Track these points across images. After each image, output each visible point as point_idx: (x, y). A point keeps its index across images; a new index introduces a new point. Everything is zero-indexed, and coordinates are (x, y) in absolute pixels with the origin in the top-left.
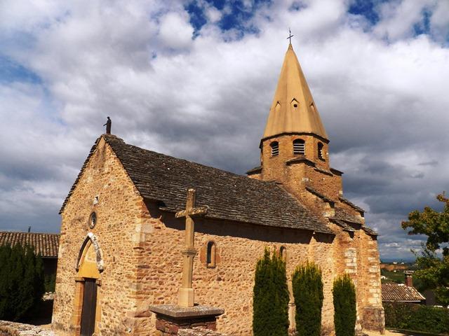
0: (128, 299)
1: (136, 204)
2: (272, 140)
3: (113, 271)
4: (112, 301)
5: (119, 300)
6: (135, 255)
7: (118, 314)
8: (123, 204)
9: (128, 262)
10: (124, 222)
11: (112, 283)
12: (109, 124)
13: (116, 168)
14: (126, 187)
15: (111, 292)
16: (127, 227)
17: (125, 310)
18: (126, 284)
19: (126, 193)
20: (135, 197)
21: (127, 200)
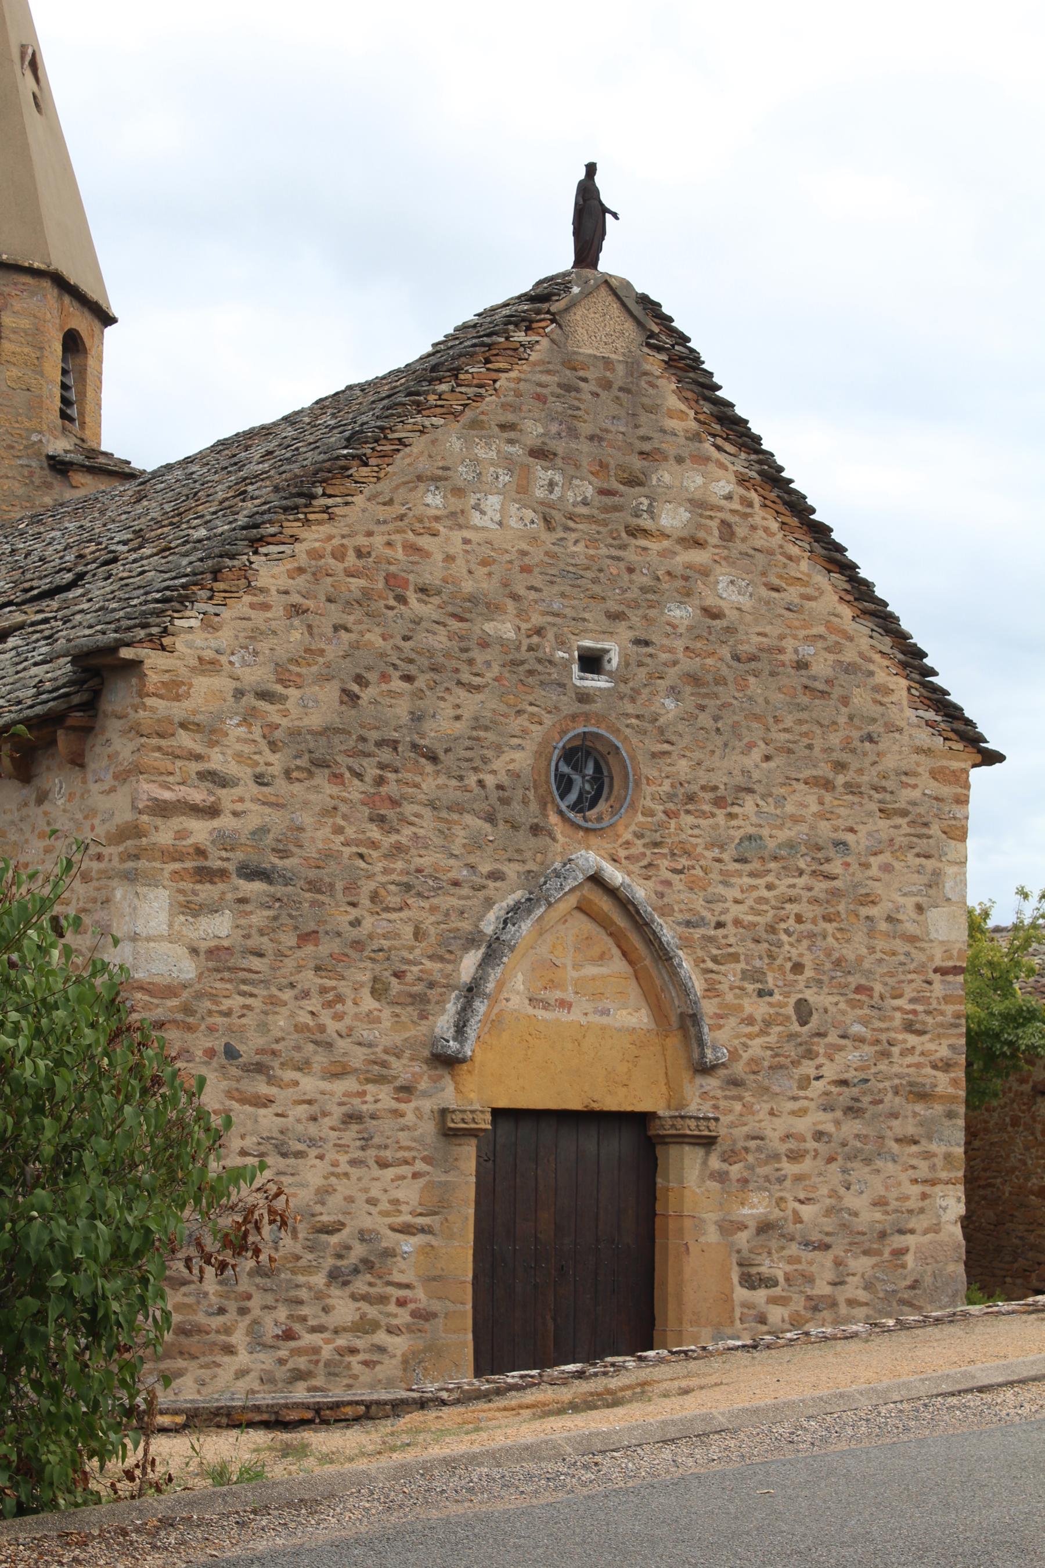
0: (916, 1190)
1: (934, 774)
3: (808, 1068)
4: (807, 1211)
5: (851, 1201)
6: (947, 999)
7: (861, 1264)
8: (848, 747)
9: (909, 1027)
11: (803, 1125)
13: (760, 540)
14: (850, 669)
15: (789, 1168)
16: (887, 868)
18: (910, 1129)
19: (861, 699)
20: (924, 737)
21: (870, 738)
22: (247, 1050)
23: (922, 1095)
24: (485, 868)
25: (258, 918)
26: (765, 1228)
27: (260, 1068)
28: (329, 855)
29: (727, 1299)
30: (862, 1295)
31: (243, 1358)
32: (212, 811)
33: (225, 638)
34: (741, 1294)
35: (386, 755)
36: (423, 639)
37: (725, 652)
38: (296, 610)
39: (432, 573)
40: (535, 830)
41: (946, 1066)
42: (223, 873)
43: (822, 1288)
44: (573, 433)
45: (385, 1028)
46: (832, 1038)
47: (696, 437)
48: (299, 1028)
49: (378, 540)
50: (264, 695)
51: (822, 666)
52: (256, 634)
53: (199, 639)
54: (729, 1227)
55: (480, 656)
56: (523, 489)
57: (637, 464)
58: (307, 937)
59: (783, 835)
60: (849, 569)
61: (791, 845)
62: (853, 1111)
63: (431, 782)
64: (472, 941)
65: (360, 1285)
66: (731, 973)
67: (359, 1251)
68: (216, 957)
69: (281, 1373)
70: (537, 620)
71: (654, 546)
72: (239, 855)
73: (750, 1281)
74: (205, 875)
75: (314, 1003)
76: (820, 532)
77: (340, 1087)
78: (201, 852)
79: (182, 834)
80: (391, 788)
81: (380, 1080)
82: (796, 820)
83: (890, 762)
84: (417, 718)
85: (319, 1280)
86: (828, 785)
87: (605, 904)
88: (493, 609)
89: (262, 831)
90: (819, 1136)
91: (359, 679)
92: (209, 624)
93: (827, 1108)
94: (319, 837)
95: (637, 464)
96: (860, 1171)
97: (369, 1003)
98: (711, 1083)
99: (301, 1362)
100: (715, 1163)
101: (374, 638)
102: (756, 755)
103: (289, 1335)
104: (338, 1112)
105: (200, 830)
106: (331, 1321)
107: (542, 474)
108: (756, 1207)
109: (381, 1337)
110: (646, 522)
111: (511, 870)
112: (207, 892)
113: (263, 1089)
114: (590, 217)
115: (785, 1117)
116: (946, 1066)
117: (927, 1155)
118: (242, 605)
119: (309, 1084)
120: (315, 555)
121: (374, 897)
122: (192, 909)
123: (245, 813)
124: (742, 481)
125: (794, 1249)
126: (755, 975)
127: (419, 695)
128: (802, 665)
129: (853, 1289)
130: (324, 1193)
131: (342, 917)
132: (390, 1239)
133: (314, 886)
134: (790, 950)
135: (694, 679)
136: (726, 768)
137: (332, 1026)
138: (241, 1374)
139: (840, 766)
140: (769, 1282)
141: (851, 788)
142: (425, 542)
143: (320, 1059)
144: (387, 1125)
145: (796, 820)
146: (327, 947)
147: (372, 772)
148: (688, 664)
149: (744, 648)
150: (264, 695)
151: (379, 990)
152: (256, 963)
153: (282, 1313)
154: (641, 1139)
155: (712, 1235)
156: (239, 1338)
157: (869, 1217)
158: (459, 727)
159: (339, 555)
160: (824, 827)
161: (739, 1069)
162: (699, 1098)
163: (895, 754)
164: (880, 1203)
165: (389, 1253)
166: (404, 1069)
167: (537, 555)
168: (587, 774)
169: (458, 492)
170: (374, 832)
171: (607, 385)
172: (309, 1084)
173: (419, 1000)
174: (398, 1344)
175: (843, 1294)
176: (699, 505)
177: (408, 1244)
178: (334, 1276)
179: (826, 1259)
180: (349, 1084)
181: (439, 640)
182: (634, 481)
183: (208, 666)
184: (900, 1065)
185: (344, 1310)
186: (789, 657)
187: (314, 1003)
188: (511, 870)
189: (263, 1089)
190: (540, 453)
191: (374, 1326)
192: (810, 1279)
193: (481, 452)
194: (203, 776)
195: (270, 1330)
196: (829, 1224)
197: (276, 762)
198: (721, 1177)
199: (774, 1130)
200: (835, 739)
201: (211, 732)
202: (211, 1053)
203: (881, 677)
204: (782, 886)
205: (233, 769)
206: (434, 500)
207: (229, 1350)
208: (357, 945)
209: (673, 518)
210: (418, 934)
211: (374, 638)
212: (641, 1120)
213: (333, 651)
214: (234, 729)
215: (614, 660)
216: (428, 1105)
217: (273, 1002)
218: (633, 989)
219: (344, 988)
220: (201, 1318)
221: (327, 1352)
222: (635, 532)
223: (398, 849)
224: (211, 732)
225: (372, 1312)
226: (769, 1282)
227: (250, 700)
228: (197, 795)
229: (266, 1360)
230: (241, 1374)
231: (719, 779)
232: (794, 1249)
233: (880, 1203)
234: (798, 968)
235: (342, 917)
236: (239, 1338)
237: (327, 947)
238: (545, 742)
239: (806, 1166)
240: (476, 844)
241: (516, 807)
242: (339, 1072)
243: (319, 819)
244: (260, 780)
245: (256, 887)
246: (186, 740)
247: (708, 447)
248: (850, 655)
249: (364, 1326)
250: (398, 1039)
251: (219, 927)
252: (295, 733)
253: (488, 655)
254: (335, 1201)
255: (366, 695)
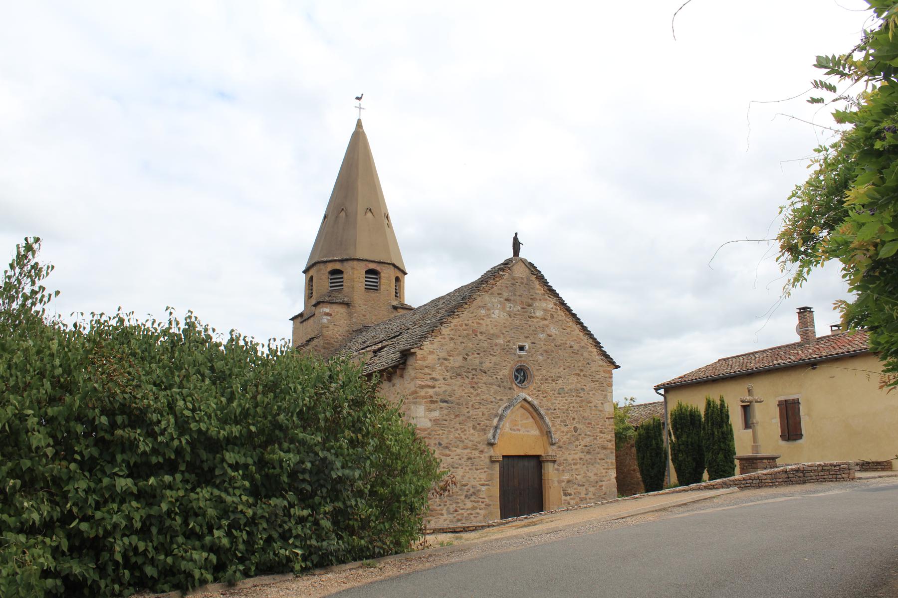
1: (604, 371)
2: (372, 266)
3: (577, 443)
5: (589, 474)
7: (592, 489)
9: (601, 432)
10: (587, 388)
11: (577, 457)
12: (516, 245)
14: (583, 347)
17: (601, 483)
19: (586, 354)
20: (601, 363)
22: (444, 443)
23: (605, 448)
24: (498, 398)
25: (445, 412)
26: (569, 481)
27: (447, 447)
28: (461, 396)
29: (560, 499)
30: (593, 497)
31: (445, 516)
32: (434, 387)
33: (435, 346)
34: (564, 497)
35: (474, 372)
36: (482, 344)
37: (553, 345)
38: (452, 339)
39: (483, 329)
40: (510, 388)
41: (610, 441)
42: (436, 402)
43: (583, 495)
44: (515, 295)
45: (476, 437)
46: (583, 435)
47: (544, 295)
48: (456, 438)
49: (470, 322)
50: (445, 359)
51: (576, 347)
52: (442, 345)
53: (429, 347)
54: (560, 482)
55: (495, 348)
56: (504, 308)
57: (530, 301)
58: (457, 416)
59: (569, 387)
60: (581, 324)
61: (571, 390)
62: (588, 453)
63: (485, 378)
64: (496, 416)
65: (472, 498)
66: (558, 421)
67: (472, 490)
68: (436, 421)
69: (455, 520)
70: (508, 339)
71: (535, 320)
72: (440, 397)
73: (566, 494)
74: (432, 402)
75: (459, 432)
76: (574, 315)
77: (466, 451)
78: (431, 397)
79: (427, 393)
80: (475, 380)
81: (476, 449)
82: (572, 384)
83: (593, 369)
84: (481, 363)
85: (463, 497)
86: (579, 375)
87: (527, 405)
88: (498, 337)
89: (446, 391)
90: (581, 459)
91: (467, 355)
92: (432, 343)
93: (582, 452)
94: (459, 392)
95: (530, 301)
96: (591, 467)
97: (472, 431)
98: (554, 447)
99: (459, 517)
100: (556, 466)
101: (470, 345)
102: (562, 369)
103: (456, 511)
104: (466, 457)
105: (431, 392)
106: (466, 507)
107: (508, 305)
108: (566, 477)
109: (478, 511)
110: (533, 315)
111: (505, 398)
112: (433, 406)
113: (448, 452)
114: (516, 245)
115: (572, 455)
116: (610, 441)
117: (607, 463)
118: (439, 338)
119: (459, 451)
120: (455, 326)
121: (472, 406)
122: (430, 410)
123: (442, 387)
124: (555, 304)
125: (576, 486)
126: (564, 421)
127: (481, 358)
128: (571, 347)
129: (590, 495)
130: (463, 477)
131: (465, 411)
132: (479, 487)
133: (458, 404)
134: (572, 415)
135: (546, 351)
136: (554, 372)
137: (464, 437)
138: (445, 520)
139: (582, 370)
140: (571, 495)
141: (585, 376)
142: (481, 322)
143: (461, 445)
144: (477, 460)
145: (572, 384)
146: (462, 418)
147: (471, 376)
148: (544, 348)
149: (558, 344)
150: (445, 359)
151: (474, 428)
152: (445, 422)
153: (454, 506)
154: (538, 461)
155: (556, 484)
156: (444, 512)
157: (594, 478)
158: (491, 365)
159: (461, 326)
160: (579, 385)
161: (561, 444)
162: (551, 451)
163: (594, 367)
164: (596, 474)
165: (479, 491)
166: (481, 447)
167: (508, 324)
168: (521, 375)
169: (488, 310)
170: (472, 390)
171: (522, 283)
172: (459, 451)
173: (484, 430)
174: (482, 512)
175: (588, 497)
176: (545, 310)
177: (483, 488)
178: (466, 496)
179: (584, 488)
180: (469, 450)
181: (485, 345)
182: (529, 306)
183: (431, 353)
184: (599, 441)
185: (469, 504)
186: (568, 345)
187: (459, 432)
188: (505, 398)
189: (448, 452)
190: (507, 300)
191: (476, 508)
192: (580, 493)
193: (493, 300)
194: (432, 379)
195: (452, 510)
196: (584, 480)
197: (448, 375)
198: (558, 470)
199: (570, 458)
200: (580, 364)
201: (433, 368)
202: (435, 444)
203: (590, 349)
204: (569, 399)
205: (438, 377)
206: (483, 312)
207: (442, 514)
208: (469, 417)
209: (539, 314)
210: (483, 414)
211: (470, 345)
212: (538, 457)
213: (461, 348)
214: (438, 368)
215: (527, 348)
216: (487, 455)
217: (449, 431)
218: (535, 426)
219: (466, 428)
220: (435, 507)
221: (465, 515)
222: (530, 317)
223: (478, 394)
224: (433, 368)
225: (476, 505)
226: (571, 495)
227: (442, 360)
228: (430, 383)
229: (451, 517)
230: (445, 520)
231: (553, 375)
232: (576, 486)
233: (596, 474)
234: (574, 419)
235: (465, 411)
236: (444, 512)
237: (462, 418)
238: (512, 368)
239: (578, 466)
240: (496, 392)
241: (505, 383)
242: (465, 448)
243: (458, 388)
244: (444, 379)
245: (445, 404)
246: (427, 370)
247: (547, 297)
248: (583, 344)
249: (474, 508)
250: (479, 439)
251: (436, 414)
252: (452, 368)
253: (498, 347)
254: (466, 478)
255: (469, 358)
